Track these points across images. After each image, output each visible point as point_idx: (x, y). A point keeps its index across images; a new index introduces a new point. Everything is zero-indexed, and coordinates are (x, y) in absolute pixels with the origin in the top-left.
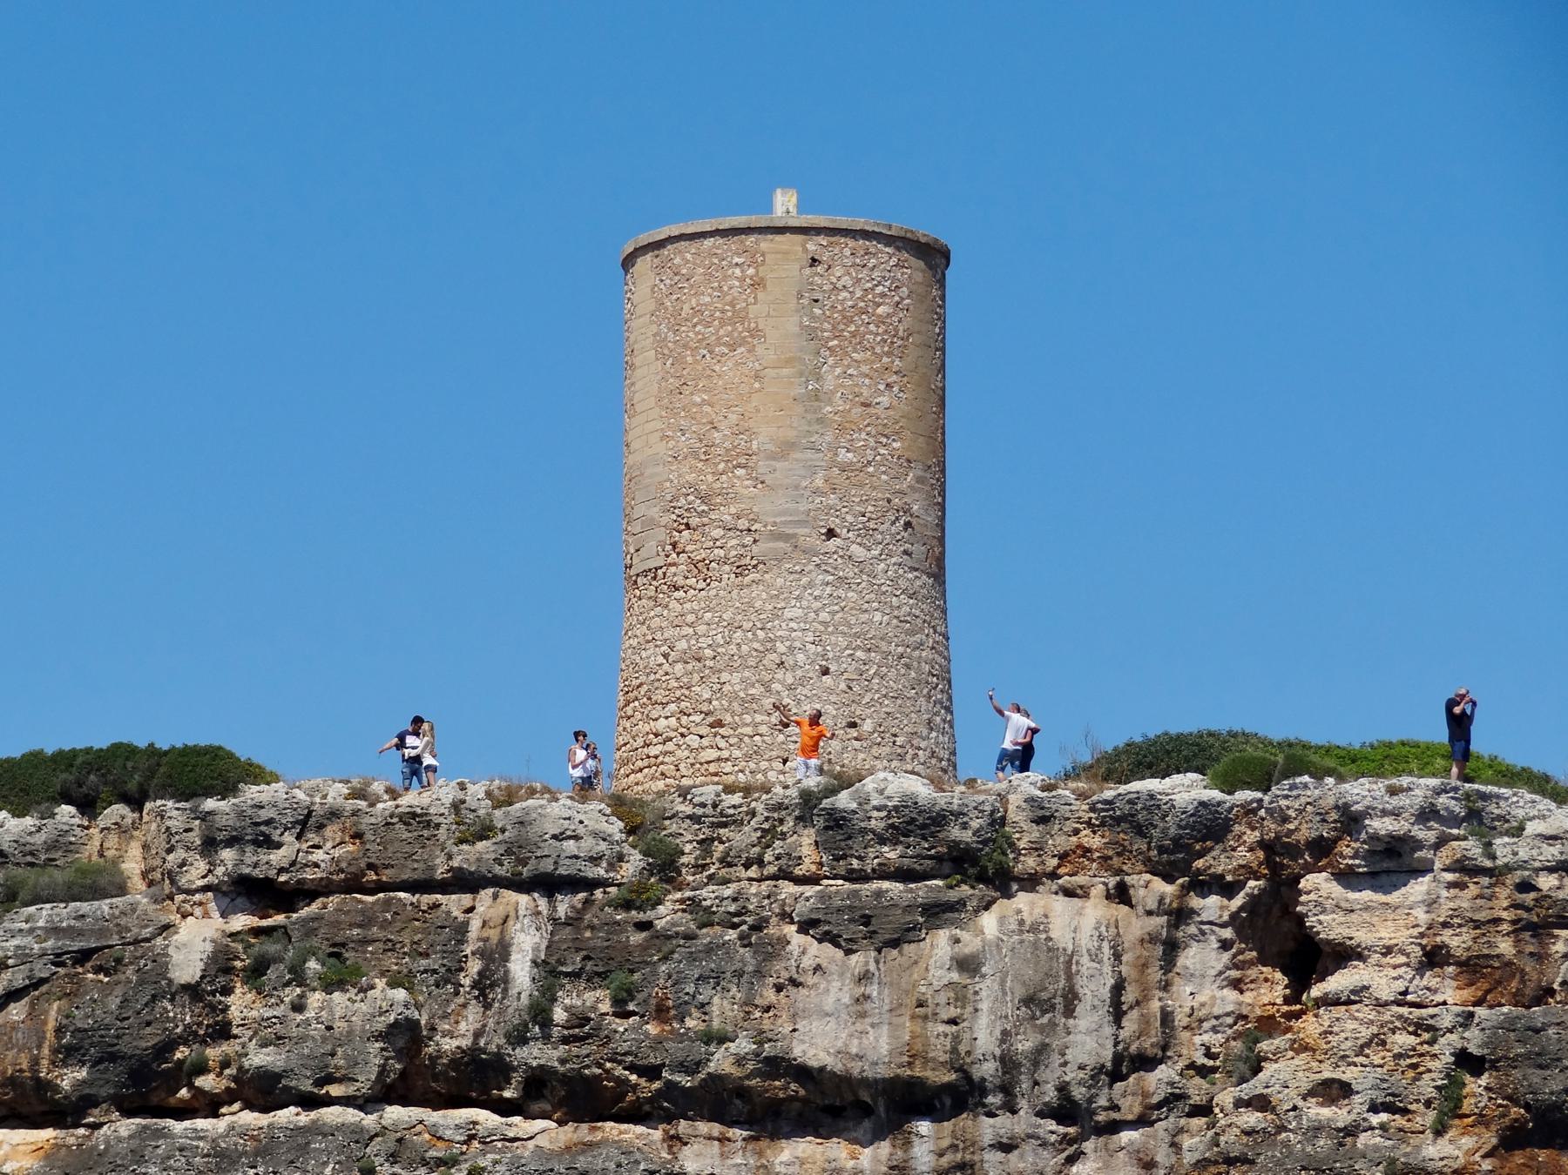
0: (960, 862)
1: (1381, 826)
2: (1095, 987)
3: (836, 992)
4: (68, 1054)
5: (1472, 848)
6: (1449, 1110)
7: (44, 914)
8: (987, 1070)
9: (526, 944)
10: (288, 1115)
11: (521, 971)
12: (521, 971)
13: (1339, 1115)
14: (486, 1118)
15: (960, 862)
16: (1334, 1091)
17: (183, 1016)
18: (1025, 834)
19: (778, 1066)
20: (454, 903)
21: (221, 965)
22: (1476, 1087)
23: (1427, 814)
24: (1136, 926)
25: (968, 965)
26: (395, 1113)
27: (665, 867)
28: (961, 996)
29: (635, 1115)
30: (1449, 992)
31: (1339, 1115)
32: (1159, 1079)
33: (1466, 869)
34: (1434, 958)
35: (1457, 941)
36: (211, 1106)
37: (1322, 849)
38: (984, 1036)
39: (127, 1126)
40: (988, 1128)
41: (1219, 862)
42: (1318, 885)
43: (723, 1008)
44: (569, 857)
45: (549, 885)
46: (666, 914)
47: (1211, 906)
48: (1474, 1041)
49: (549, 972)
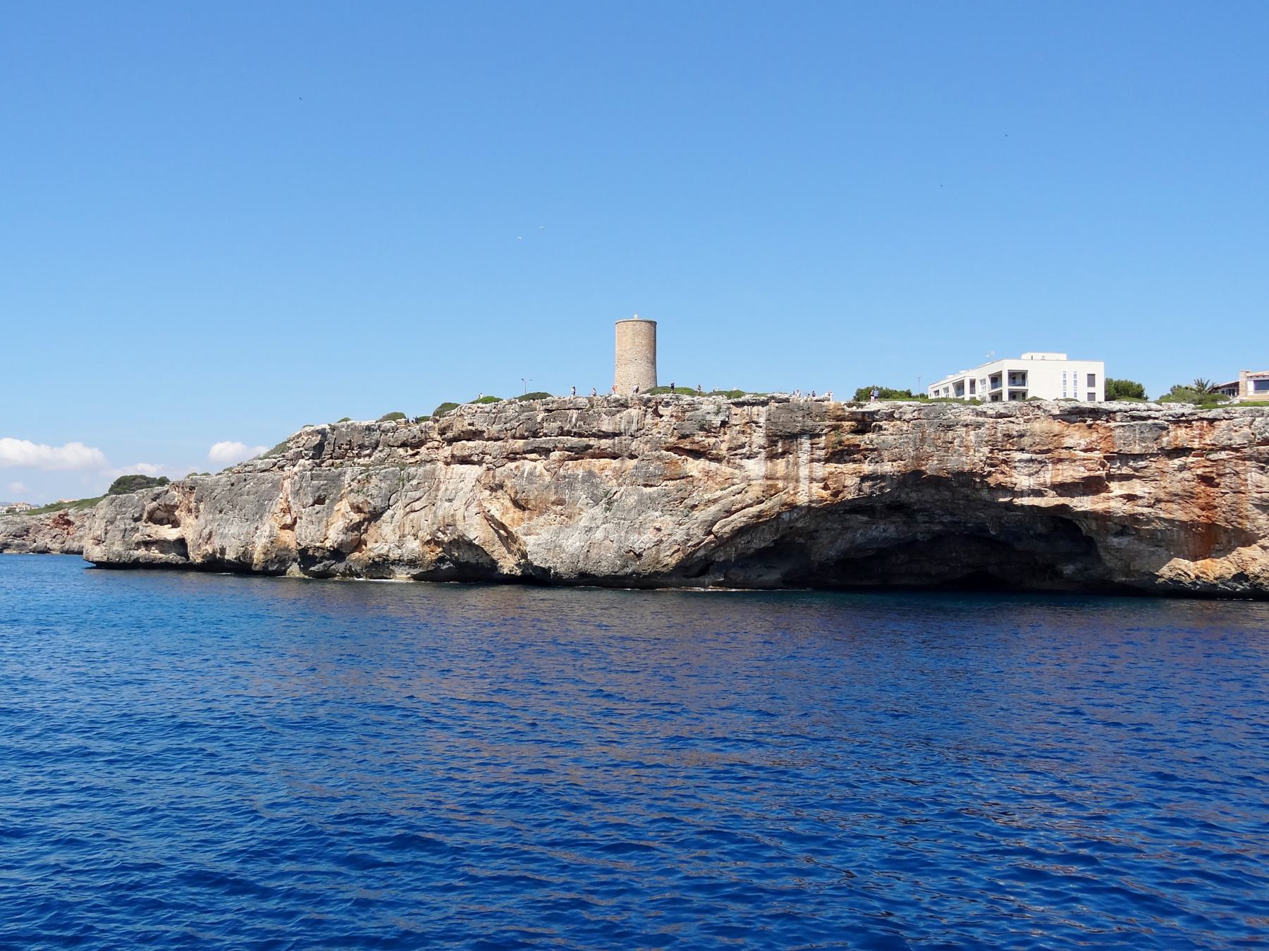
0: (622, 405)
1: (665, 400)
2: (635, 421)
3: (607, 422)
4: (526, 431)
5: (677, 402)
6: (672, 435)
7: (526, 414)
8: (623, 431)
9: (575, 416)
10: (548, 438)
11: (574, 420)
12: (574, 420)
13: (660, 436)
14: (569, 438)
15: (622, 405)
16: (659, 433)
17: (539, 426)
18: (630, 401)
19: (599, 431)
20: (568, 411)
21: (543, 420)
22: (675, 431)
23: (671, 398)
24: (641, 412)
25: (621, 418)
26: (560, 437)
27: (592, 406)
28: (620, 422)
29: (586, 437)
30: (674, 420)
31: (660, 436)
32: (642, 432)
33: (676, 405)
34: (672, 416)
35: (674, 414)
36: (541, 437)
37: (660, 403)
38: (622, 427)
39: (532, 439)
40: (623, 438)
41: (650, 404)
42: (660, 407)
43: (595, 424)
44: (580, 406)
45: (578, 409)
46: (590, 412)
47: (650, 410)
48: (675, 426)
49: (577, 420)
